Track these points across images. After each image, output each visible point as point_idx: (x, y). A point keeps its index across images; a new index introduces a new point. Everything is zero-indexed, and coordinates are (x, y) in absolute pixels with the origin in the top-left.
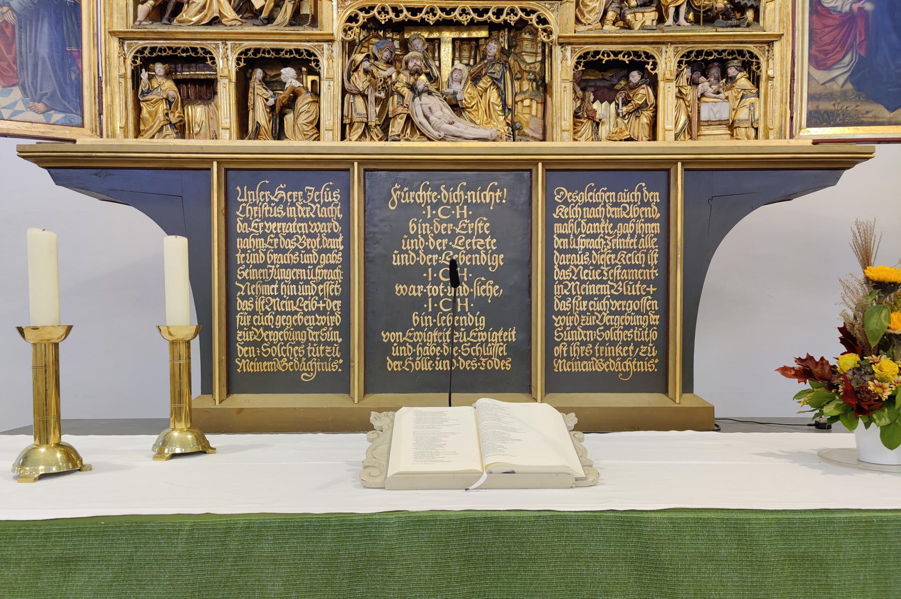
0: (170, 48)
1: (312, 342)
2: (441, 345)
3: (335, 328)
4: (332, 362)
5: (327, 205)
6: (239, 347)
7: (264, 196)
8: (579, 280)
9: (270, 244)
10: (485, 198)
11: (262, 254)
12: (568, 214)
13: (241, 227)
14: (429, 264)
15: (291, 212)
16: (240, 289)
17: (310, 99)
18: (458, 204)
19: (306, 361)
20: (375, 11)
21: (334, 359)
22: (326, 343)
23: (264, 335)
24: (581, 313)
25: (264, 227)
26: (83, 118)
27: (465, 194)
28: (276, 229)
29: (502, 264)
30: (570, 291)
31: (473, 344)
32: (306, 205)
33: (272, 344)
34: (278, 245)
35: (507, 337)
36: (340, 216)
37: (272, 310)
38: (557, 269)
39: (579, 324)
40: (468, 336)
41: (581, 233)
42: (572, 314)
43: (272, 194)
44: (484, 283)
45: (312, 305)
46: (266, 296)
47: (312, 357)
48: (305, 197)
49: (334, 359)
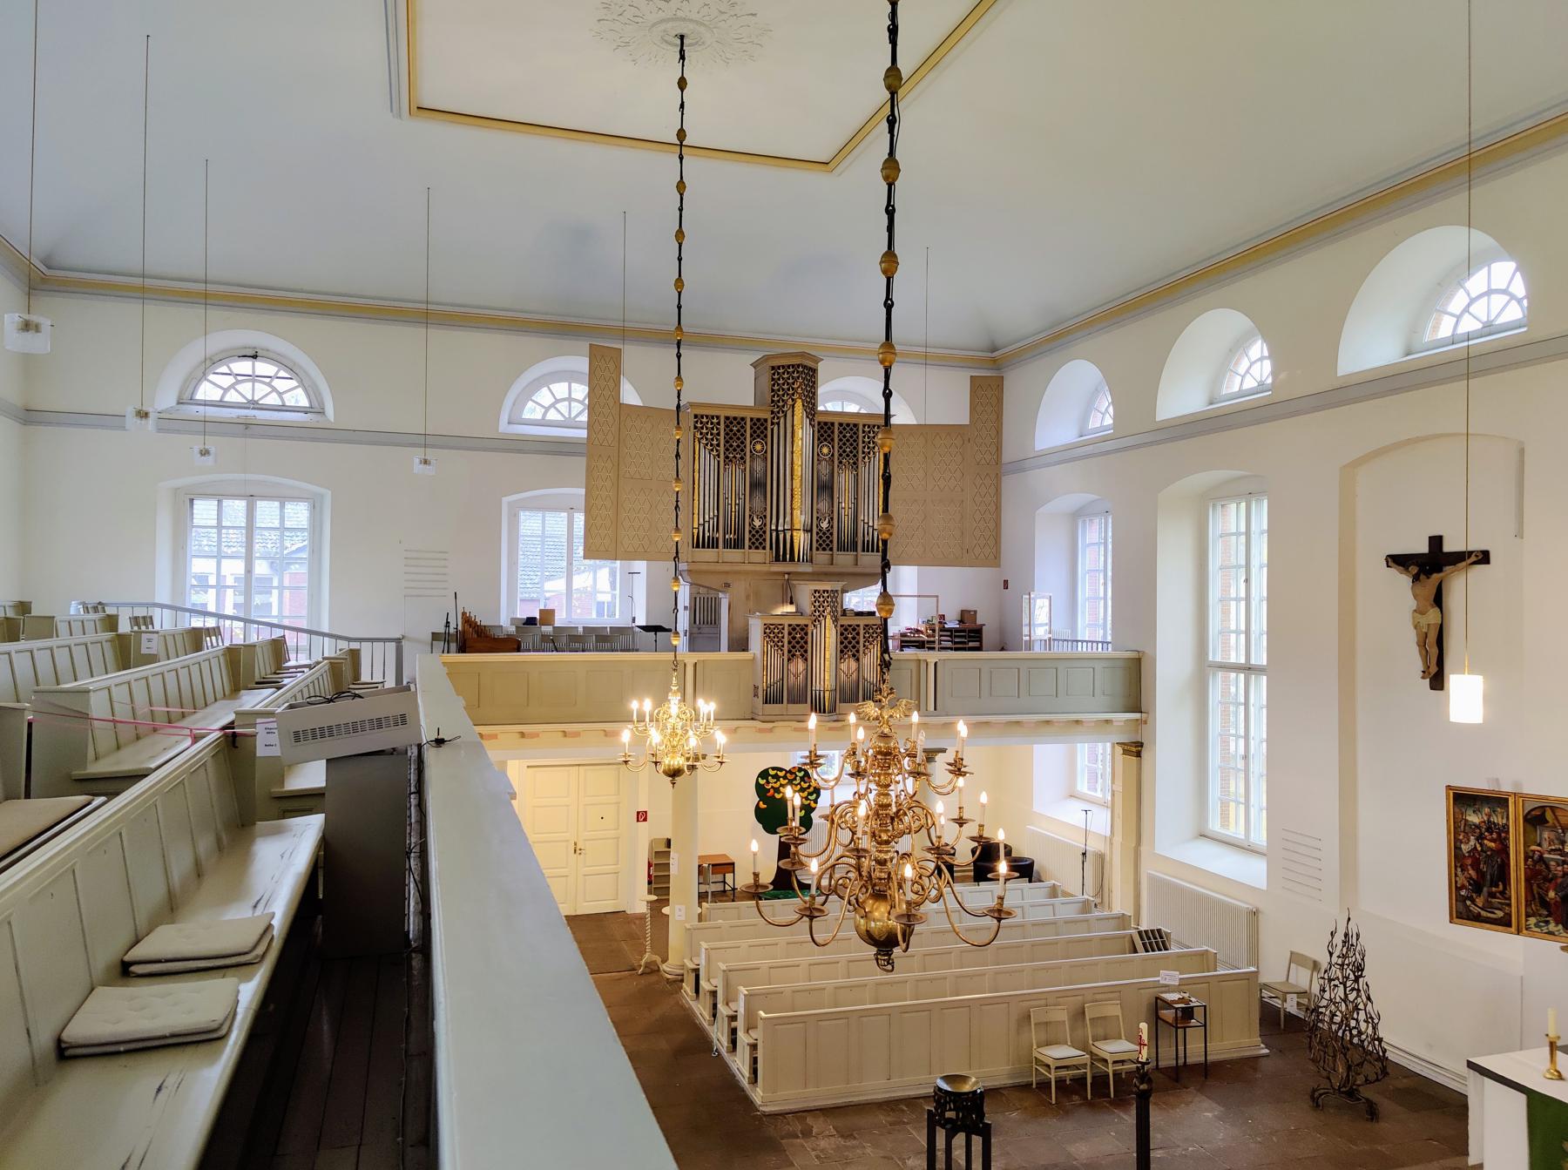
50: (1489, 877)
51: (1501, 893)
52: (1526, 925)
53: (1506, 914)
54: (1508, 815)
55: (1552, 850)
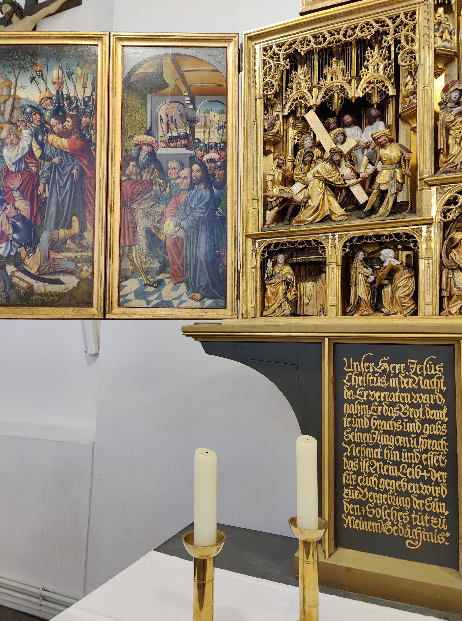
0: (289, 243)
1: (416, 510)
3: (441, 499)
4: (438, 533)
5: (430, 377)
6: (345, 504)
7: (368, 368)
9: (373, 411)
11: (366, 420)
13: (347, 394)
15: (394, 383)
16: (346, 450)
17: (408, 275)
21: (440, 531)
22: (431, 514)
23: (369, 495)
25: (368, 395)
26: (226, 301)
28: (379, 397)
32: (409, 377)
33: (376, 506)
34: (382, 412)
36: (444, 389)
37: (376, 473)
43: (376, 365)
45: (416, 473)
46: (370, 459)
47: (417, 525)
48: (407, 369)
49: (440, 531)
50: (53, 209)
51: (73, 238)
52: (119, 297)
53: (82, 280)
54: (95, 79)
55: (172, 139)
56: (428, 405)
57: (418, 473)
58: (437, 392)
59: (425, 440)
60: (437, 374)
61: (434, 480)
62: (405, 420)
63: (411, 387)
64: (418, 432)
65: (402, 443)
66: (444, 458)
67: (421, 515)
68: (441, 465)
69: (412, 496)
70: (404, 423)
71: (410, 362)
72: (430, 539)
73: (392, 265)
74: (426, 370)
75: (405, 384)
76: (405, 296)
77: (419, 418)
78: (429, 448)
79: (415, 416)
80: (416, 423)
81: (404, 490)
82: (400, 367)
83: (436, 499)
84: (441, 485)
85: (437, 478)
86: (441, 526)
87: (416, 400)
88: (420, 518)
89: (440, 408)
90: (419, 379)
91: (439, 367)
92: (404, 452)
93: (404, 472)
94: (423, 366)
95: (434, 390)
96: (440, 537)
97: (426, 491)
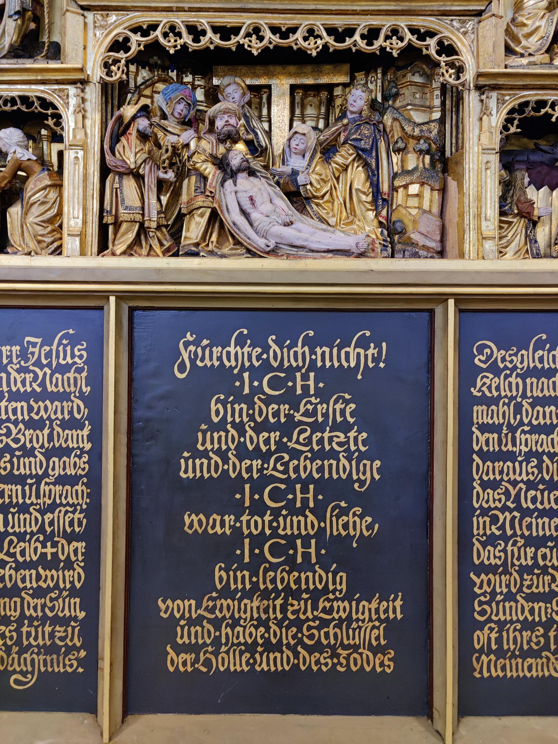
1: (31, 619)
2: (265, 624)
3: (73, 592)
4: (66, 654)
5: (63, 369)
8: (519, 508)
10: (347, 360)
12: (498, 388)
14: (246, 476)
18: (298, 369)
19: (19, 653)
20: (158, 33)
21: (70, 649)
22: (56, 621)
24: (523, 570)
27: (313, 352)
29: (377, 477)
30: (502, 528)
31: (325, 623)
32: (25, 370)
35: (386, 611)
36: (87, 390)
38: (478, 488)
39: (520, 590)
40: (315, 607)
41: (521, 424)
42: (506, 572)
44: (344, 512)
47: (30, 646)
48: (24, 355)
49: (70, 649)
56: (59, 423)
57: (36, 549)
58: (75, 396)
59: (51, 487)
60: (75, 363)
61: (62, 558)
62: (17, 453)
63: (29, 389)
64: (40, 472)
65: (10, 497)
66: (82, 516)
67: (39, 626)
68: (77, 529)
69: (23, 594)
70: (15, 460)
71: (29, 342)
72: (52, 666)
73: (17, 159)
74: (58, 357)
75: (19, 384)
76: (43, 221)
77: (42, 447)
78: (58, 501)
79: (36, 445)
80: (35, 457)
81: (9, 585)
82: (11, 351)
83: (65, 593)
84: (75, 566)
85: (69, 553)
86: (72, 640)
87: (37, 413)
88: (37, 632)
89: (79, 425)
90: (45, 374)
91: (79, 350)
92: (13, 514)
93: (12, 551)
94: (51, 350)
95: (70, 393)
96: (70, 660)
97: (49, 581)
